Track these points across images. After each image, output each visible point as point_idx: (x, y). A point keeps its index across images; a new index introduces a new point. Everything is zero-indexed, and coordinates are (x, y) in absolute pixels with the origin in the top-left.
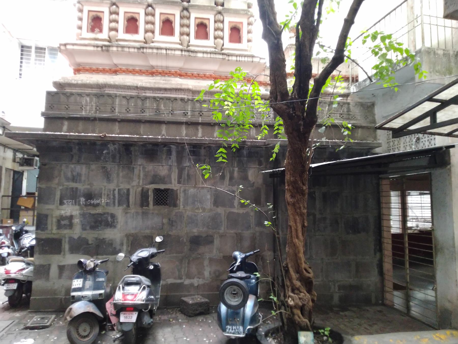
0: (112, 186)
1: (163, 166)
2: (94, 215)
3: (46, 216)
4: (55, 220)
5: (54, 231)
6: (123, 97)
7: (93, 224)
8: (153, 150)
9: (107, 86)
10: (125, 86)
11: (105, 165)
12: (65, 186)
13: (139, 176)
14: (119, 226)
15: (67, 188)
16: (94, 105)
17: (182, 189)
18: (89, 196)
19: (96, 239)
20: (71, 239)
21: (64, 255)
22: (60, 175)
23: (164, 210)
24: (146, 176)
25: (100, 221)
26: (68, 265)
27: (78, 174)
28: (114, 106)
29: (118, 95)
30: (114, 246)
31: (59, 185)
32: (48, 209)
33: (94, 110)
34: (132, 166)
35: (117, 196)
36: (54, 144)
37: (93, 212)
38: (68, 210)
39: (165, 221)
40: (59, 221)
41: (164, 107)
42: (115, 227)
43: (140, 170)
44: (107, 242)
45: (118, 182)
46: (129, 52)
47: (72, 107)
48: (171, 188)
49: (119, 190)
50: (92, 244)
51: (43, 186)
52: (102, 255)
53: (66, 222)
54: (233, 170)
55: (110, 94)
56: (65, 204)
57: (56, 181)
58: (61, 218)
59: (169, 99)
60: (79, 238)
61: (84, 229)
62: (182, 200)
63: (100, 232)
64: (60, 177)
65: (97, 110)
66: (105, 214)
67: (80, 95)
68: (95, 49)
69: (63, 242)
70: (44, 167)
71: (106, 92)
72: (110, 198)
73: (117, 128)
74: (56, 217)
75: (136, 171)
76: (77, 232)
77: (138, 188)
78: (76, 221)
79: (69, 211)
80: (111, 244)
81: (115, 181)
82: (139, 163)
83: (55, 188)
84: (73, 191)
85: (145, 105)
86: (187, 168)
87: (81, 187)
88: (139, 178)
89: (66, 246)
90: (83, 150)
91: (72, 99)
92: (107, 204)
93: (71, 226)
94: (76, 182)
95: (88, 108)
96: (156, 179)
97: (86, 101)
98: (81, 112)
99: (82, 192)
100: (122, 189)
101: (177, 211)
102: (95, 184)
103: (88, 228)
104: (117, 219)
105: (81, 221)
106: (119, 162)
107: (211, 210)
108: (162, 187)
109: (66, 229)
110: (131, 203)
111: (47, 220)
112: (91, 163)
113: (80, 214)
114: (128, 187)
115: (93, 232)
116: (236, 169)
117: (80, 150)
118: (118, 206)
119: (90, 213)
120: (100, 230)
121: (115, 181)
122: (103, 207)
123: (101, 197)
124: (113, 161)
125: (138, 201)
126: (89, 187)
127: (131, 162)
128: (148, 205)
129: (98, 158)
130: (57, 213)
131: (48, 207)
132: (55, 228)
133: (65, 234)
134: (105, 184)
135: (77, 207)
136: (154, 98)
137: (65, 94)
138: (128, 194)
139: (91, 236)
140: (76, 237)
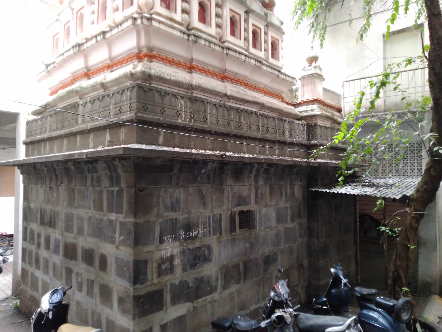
0: (207, 213)
1: (245, 185)
2: (193, 250)
3: (146, 262)
4: (155, 265)
6: (213, 104)
7: (192, 261)
8: (240, 169)
9: (200, 88)
10: (216, 91)
11: (201, 188)
12: (165, 218)
13: (228, 198)
15: (167, 221)
16: (189, 111)
17: (258, 209)
18: (188, 228)
19: (196, 279)
20: (172, 285)
22: (158, 203)
23: (246, 232)
24: (233, 197)
25: (197, 258)
27: (177, 200)
28: (206, 114)
29: (209, 101)
30: (211, 284)
31: (158, 217)
32: (147, 252)
33: (189, 117)
34: (222, 187)
36: (158, 162)
37: (192, 247)
39: (248, 245)
40: (159, 266)
41: (244, 120)
43: (229, 192)
44: (205, 281)
45: (212, 207)
47: (168, 111)
48: (251, 209)
49: (213, 216)
50: (192, 287)
51: (141, 221)
52: (201, 297)
53: (166, 266)
54: (287, 187)
55: (203, 99)
57: (155, 212)
58: (163, 261)
59: (247, 111)
60: (181, 282)
61: (184, 270)
62: (258, 220)
63: (199, 270)
64: (159, 206)
65: (192, 118)
66: (203, 246)
67: (175, 96)
68: (182, 35)
69: (165, 293)
70: (140, 193)
71: (194, 95)
72: (206, 227)
74: (156, 261)
75: (226, 192)
76: (178, 276)
77: (227, 212)
78: (177, 261)
79: (170, 250)
80: (209, 282)
81: (210, 206)
82: (228, 184)
83: (154, 222)
84: (173, 223)
85: (230, 117)
87: (180, 216)
88: (228, 202)
89: (168, 297)
90: (184, 169)
91: (167, 99)
92: (204, 235)
93: (171, 270)
94: (175, 212)
95: (183, 114)
96: (241, 201)
97: (181, 104)
98: (177, 119)
99: (181, 223)
100: (216, 215)
101: (255, 233)
102: (193, 212)
103: (188, 268)
104: (212, 251)
105: (182, 261)
106: (213, 183)
107: (276, 227)
109: (167, 274)
111: (146, 268)
112: (189, 185)
113: (181, 252)
114: (220, 212)
115: (193, 271)
116: (288, 186)
117: (181, 170)
119: (189, 249)
120: (199, 268)
121: (210, 206)
122: (201, 238)
123: (198, 227)
124: (208, 183)
125: (228, 228)
126: (187, 216)
127: (223, 183)
128: (235, 231)
129: (194, 180)
130: (157, 256)
131: (147, 249)
132: (155, 276)
133: (167, 281)
134: (202, 210)
135: (177, 243)
136: (237, 109)
137: (160, 92)
138: (220, 221)
139: (190, 277)
140: (177, 282)
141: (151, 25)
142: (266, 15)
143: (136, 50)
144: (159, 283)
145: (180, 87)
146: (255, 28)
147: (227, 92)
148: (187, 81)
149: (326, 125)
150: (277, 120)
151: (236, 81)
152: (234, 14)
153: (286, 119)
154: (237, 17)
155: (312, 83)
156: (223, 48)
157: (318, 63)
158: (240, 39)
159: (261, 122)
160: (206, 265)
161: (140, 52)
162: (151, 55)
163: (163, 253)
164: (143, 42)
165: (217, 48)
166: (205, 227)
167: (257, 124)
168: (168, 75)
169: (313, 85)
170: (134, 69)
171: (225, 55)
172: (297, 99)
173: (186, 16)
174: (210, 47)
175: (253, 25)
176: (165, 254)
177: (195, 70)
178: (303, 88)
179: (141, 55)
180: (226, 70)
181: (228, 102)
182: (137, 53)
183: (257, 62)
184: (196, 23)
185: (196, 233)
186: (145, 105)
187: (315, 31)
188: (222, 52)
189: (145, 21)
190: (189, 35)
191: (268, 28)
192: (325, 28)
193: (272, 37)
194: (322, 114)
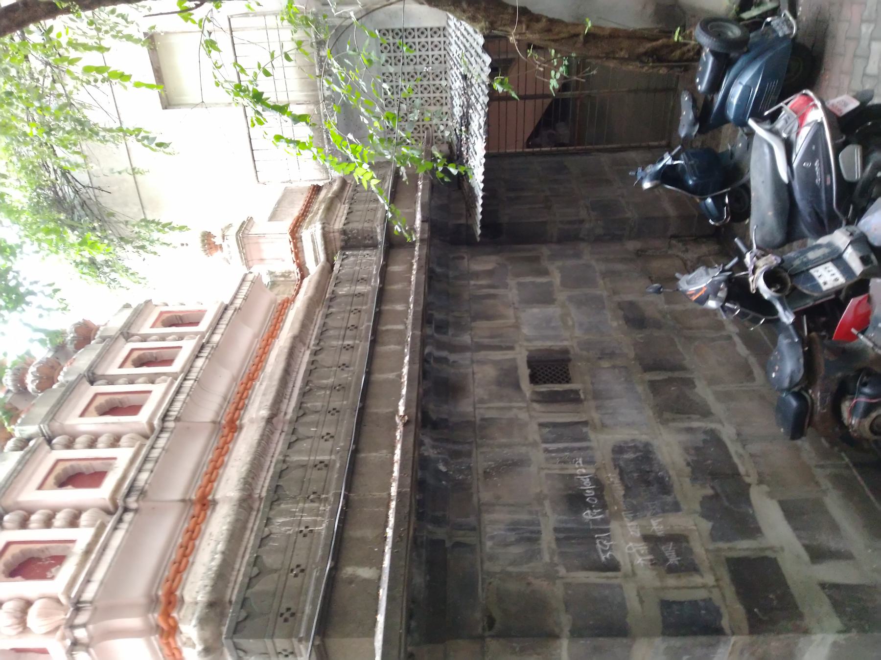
0: (537, 456)
1: (473, 373)
2: (627, 489)
3: (666, 605)
4: (671, 581)
5: (709, 579)
6: (289, 448)
7: (654, 489)
8: (437, 385)
9: (250, 480)
11: (481, 471)
12: (556, 559)
13: (502, 409)
14: (644, 438)
15: (562, 554)
16: (301, 505)
17: (526, 344)
18: (575, 500)
19: (694, 479)
20: (715, 535)
21: (771, 548)
22: (521, 577)
23: (578, 368)
24: (501, 398)
25: (643, 477)
26: (799, 537)
28: (311, 463)
29: (281, 458)
30: (701, 445)
31: (555, 576)
32: (641, 602)
33: (316, 505)
35: (561, 445)
36: (419, 580)
37: (619, 490)
38: (630, 549)
39: (605, 364)
40: (672, 570)
41: (329, 378)
42: (647, 444)
43: (489, 408)
44: (695, 458)
45: (524, 445)
46: (163, 449)
47: (300, 558)
48: (525, 359)
49: (545, 441)
50: (713, 488)
51: (565, 621)
52: (734, 467)
54: (474, 285)
55: (274, 473)
56: (611, 555)
57: (541, 585)
58: (658, 561)
59: (309, 372)
60: (705, 516)
61: (676, 507)
62: (548, 344)
63: (672, 473)
65: (319, 498)
66: (616, 466)
67: (263, 541)
68: (124, 526)
69: (735, 554)
70: (497, 625)
71: (264, 494)
73: (374, 454)
75: (489, 415)
76: (691, 523)
77: (534, 410)
78: (657, 526)
79: (631, 544)
80: (697, 449)
81: (523, 450)
85: (318, 409)
86: (475, 340)
87: (550, 520)
89: (744, 547)
90: (439, 514)
91: (270, 560)
92: (589, 462)
93: (678, 539)
94: (539, 532)
95: (307, 519)
96: (508, 379)
97: (284, 524)
98: (319, 533)
99: (565, 517)
100: (541, 436)
101: (577, 350)
102: (538, 490)
103: (669, 499)
104: (626, 442)
105: (654, 515)
107: (563, 306)
108: (524, 372)
109: (690, 551)
110: (576, 419)
111: (681, 603)
112: (475, 499)
113: (635, 518)
114: (536, 427)
115: (676, 486)
116: (472, 282)
117: (438, 522)
118: (590, 440)
119: (624, 496)
120: (667, 472)
121: (523, 450)
122: (598, 469)
123: (572, 476)
124: (469, 454)
126: (547, 503)
127: (468, 422)
128: (576, 392)
129: (463, 488)
130: (648, 576)
132: (697, 580)
133: (707, 550)
134: (533, 469)
135: (614, 526)
136: (304, 394)
137: (250, 579)
138: (555, 425)
139: (691, 492)
140: (706, 525)
141: (91, 602)
142: (103, 339)
143: (153, 638)
144: (712, 569)
145: (244, 528)
146: (129, 362)
147: (263, 418)
148: (231, 512)
149: (345, 212)
150: (331, 310)
151: (241, 399)
152: (92, 408)
153: (329, 291)
154: (101, 400)
155: (257, 243)
156: (162, 430)
157: (217, 232)
158: (149, 392)
159: (334, 343)
160: (660, 457)
161: (158, 629)
162: (166, 601)
163: (639, 561)
164: (135, 622)
165: (161, 443)
166: (572, 460)
167: (339, 350)
168: (213, 559)
169: (261, 240)
170: (194, 646)
171: (178, 424)
172: (290, 272)
173: (84, 518)
174: (158, 458)
175: (121, 366)
176: (641, 555)
177: (209, 493)
178: (266, 262)
179: (165, 627)
180: (214, 422)
181: (285, 414)
182: (161, 636)
183: (202, 355)
184: (101, 494)
185: (587, 481)
186: (282, 615)
187: (152, 242)
188: (172, 432)
189: (82, 618)
190: (126, 510)
191: (133, 335)
192: (147, 222)
193: (153, 326)
194: (321, 220)
